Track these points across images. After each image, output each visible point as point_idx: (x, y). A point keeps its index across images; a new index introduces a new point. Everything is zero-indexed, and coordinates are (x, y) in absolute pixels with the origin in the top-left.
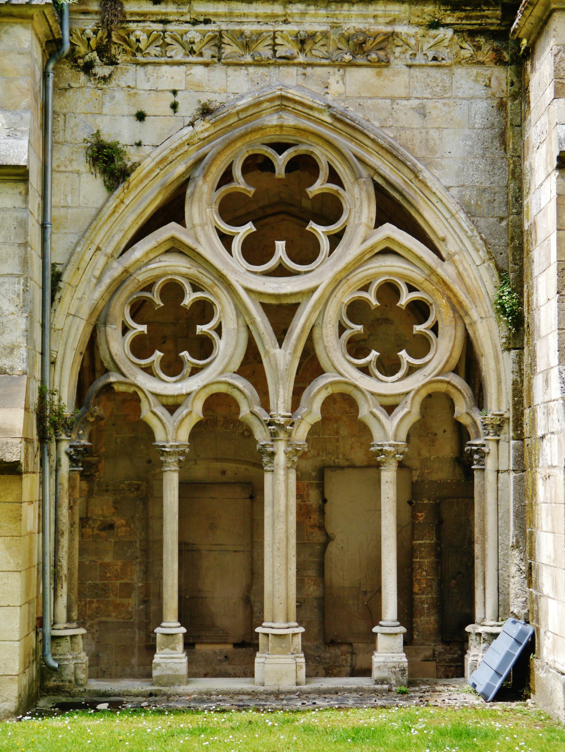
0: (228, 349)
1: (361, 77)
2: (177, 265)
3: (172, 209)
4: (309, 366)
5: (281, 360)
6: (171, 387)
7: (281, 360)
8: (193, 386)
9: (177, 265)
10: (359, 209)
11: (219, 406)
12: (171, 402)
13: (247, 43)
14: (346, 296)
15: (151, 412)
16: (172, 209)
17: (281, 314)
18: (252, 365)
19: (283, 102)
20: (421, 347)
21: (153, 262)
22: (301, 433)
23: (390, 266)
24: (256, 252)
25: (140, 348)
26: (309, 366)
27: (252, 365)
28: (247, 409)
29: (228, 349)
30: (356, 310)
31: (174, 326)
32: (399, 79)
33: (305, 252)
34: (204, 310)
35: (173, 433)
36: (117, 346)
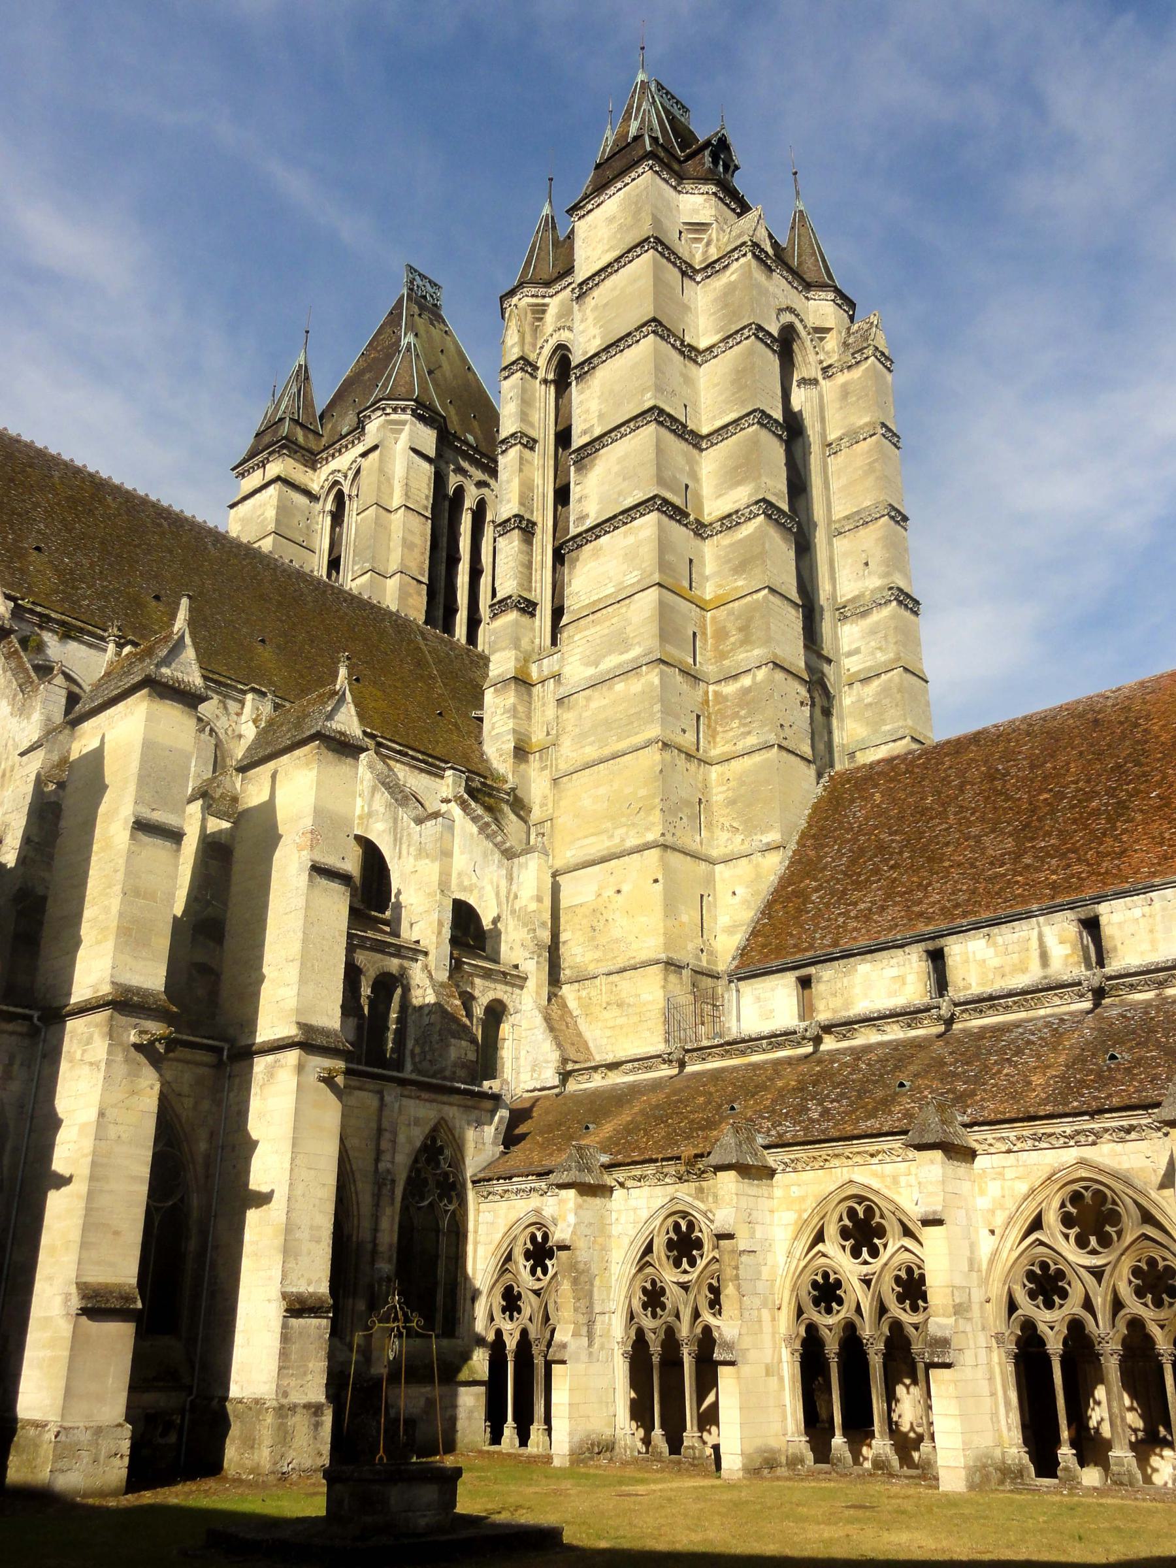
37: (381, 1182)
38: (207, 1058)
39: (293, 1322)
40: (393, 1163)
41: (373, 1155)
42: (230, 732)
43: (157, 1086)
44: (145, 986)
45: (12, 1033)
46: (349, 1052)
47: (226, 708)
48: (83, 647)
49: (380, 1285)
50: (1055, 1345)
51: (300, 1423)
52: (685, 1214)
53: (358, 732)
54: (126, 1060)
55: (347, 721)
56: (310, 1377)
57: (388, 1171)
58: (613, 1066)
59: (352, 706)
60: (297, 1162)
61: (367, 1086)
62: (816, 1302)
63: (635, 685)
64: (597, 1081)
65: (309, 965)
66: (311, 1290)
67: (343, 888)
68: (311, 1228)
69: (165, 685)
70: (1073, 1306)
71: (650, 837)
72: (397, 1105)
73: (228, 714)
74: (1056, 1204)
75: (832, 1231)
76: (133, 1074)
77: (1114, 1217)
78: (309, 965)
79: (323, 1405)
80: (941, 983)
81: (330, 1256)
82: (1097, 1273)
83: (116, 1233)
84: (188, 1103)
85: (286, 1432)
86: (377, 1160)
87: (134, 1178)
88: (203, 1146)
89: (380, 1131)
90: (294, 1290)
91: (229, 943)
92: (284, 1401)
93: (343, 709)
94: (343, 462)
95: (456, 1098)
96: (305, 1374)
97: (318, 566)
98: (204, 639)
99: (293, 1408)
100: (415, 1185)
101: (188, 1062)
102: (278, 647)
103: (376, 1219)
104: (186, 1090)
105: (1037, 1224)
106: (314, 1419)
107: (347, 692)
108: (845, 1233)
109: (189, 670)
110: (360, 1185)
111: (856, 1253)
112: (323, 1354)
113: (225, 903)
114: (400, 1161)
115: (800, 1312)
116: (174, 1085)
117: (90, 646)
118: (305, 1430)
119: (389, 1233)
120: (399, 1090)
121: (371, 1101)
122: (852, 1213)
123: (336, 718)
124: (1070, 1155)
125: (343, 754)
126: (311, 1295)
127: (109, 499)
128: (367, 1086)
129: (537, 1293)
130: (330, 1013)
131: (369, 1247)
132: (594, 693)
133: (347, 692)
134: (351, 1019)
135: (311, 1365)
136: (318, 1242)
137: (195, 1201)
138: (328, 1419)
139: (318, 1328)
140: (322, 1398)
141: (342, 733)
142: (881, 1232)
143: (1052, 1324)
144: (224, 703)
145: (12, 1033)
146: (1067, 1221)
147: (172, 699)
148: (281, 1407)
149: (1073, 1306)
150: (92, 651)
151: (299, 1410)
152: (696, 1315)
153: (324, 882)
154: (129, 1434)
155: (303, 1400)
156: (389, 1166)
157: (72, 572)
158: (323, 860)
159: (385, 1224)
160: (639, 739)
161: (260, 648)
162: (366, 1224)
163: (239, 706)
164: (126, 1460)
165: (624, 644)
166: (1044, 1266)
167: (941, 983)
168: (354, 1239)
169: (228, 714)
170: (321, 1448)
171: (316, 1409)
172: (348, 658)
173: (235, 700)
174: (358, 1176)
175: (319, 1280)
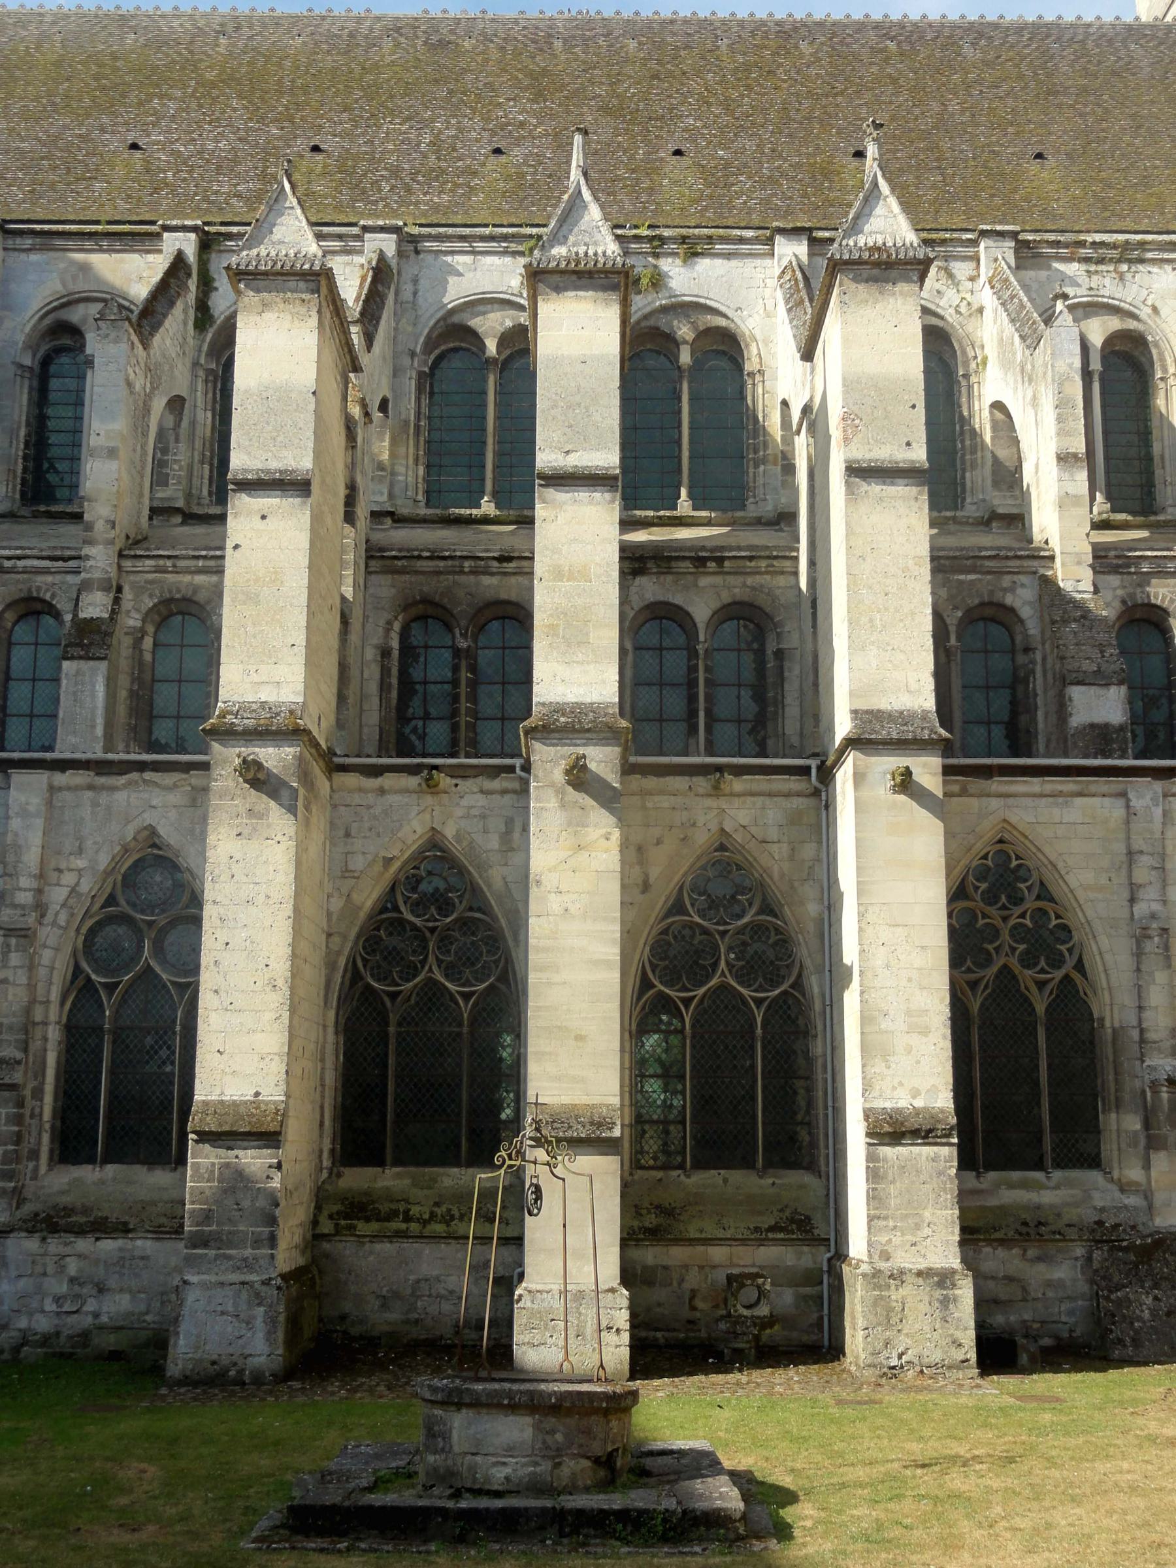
39: (887, 1151)
40: (1165, 902)
41: (1126, 895)
42: (963, 309)
43: (616, 834)
44: (588, 700)
45: (504, 792)
46: (946, 740)
47: (951, 276)
48: (718, 262)
49: (1156, 1092)
51: (915, 1299)
53: (911, 237)
54: (563, 805)
55: (889, 225)
56: (927, 1231)
57: (1153, 916)
59: (893, 202)
60: (870, 917)
61: (1093, 788)
65: (864, 620)
66: (919, 1103)
67: (914, 490)
68: (909, 1013)
69: (557, 271)
72: (1158, 812)
73: (957, 284)
76: (576, 824)
78: (864, 620)
79: (954, 1272)
81: (949, 1053)
83: (580, 1038)
84: (779, 851)
85: (890, 1310)
86: (1132, 900)
87: (596, 963)
88: (812, 909)
90: (888, 1105)
92: (883, 1265)
93: (879, 210)
96: (918, 1227)
98: (934, 187)
99: (899, 1276)
101: (770, 795)
102: (1069, 156)
103: (1139, 992)
104: (773, 834)
106: (938, 1293)
107: (881, 182)
109: (598, 237)
110: (1104, 942)
112: (949, 1196)
116: (753, 830)
117: (728, 256)
118: (924, 1307)
120: (1158, 786)
121: (1113, 811)
123: (867, 228)
125: (887, 281)
126: (917, 1112)
127: (803, 45)
128: (1093, 788)
130: (914, 686)
131: (1135, 1034)
133: (881, 182)
134: (1113, 689)
135: (927, 1214)
136: (925, 1032)
137: (814, 984)
138: (965, 1293)
139: (934, 1160)
140: (955, 1263)
141: (876, 249)
144: (946, 269)
145: (504, 792)
147: (577, 288)
148: (877, 1273)
150: (734, 263)
151: (909, 1278)
153: (875, 489)
154: (625, 1303)
155: (922, 1265)
156: (1156, 907)
157: (727, 165)
158: (868, 456)
161: (1035, 165)
162: (1126, 999)
163: (973, 265)
164: (626, 1337)
168: (1108, 1024)
169: (957, 284)
170: (959, 1335)
171: (944, 1279)
172: (878, 126)
173: (965, 258)
174: (1098, 927)
175: (934, 1090)
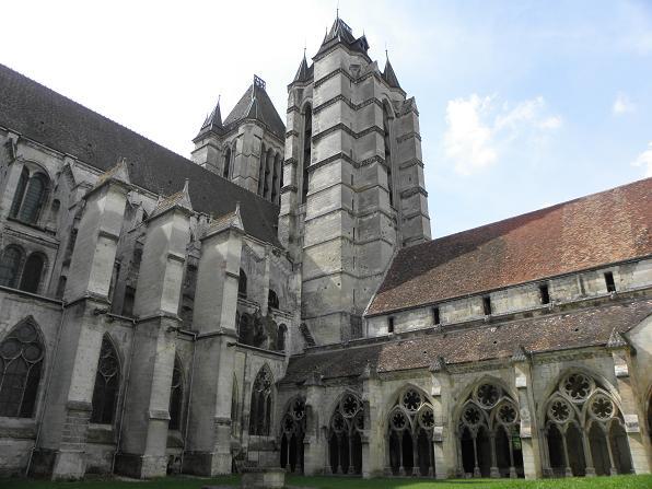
0: (571, 414)
1: (587, 361)
2: (558, 399)
3: (557, 389)
4: (588, 416)
5: (582, 416)
6: (561, 422)
7: (582, 416)
8: (566, 421)
9: (558, 399)
10: (593, 386)
11: (571, 425)
12: (563, 424)
13: (564, 357)
14: (592, 403)
15: (559, 428)
16: (557, 389)
17: (580, 406)
18: (576, 417)
19: (573, 367)
20: (610, 411)
21: (555, 399)
22: (588, 429)
23: (599, 396)
24: (574, 395)
25: (555, 415)
26: (588, 416)
27: (576, 417)
28: (577, 425)
29: (571, 414)
30: (595, 404)
31: (560, 410)
32: (595, 360)
33: (583, 394)
34: (565, 407)
35: (563, 431)
36: (550, 415)
37: (245, 383)
38: (190, 338)
50: (474, 435)
52: (350, 396)
58: (324, 347)
62: (395, 424)
63: (333, 217)
64: (318, 353)
70: (481, 423)
71: (337, 269)
74: (476, 390)
75: (401, 400)
77: (496, 394)
80: (437, 320)
82: (489, 412)
89: (246, 366)
91: (196, 299)
94: (231, 139)
95: (271, 356)
97: (221, 173)
100: (257, 385)
103: (244, 395)
105: (470, 396)
108: (406, 401)
111: (409, 408)
113: (195, 287)
114: (251, 378)
115: (390, 426)
119: (248, 402)
122: (408, 394)
124: (481, 374)
129: (298, 422)
132: (319, 220)
142: (419, 400)
143: (473, 428)
146: (480, 395)
149: (481, 423)
152: (354, 428)
159: (247, 397)
160: (334, 236)
162: (241, 397)
165: (329, 203)
166: (472, 410)
167: (437, 320)
